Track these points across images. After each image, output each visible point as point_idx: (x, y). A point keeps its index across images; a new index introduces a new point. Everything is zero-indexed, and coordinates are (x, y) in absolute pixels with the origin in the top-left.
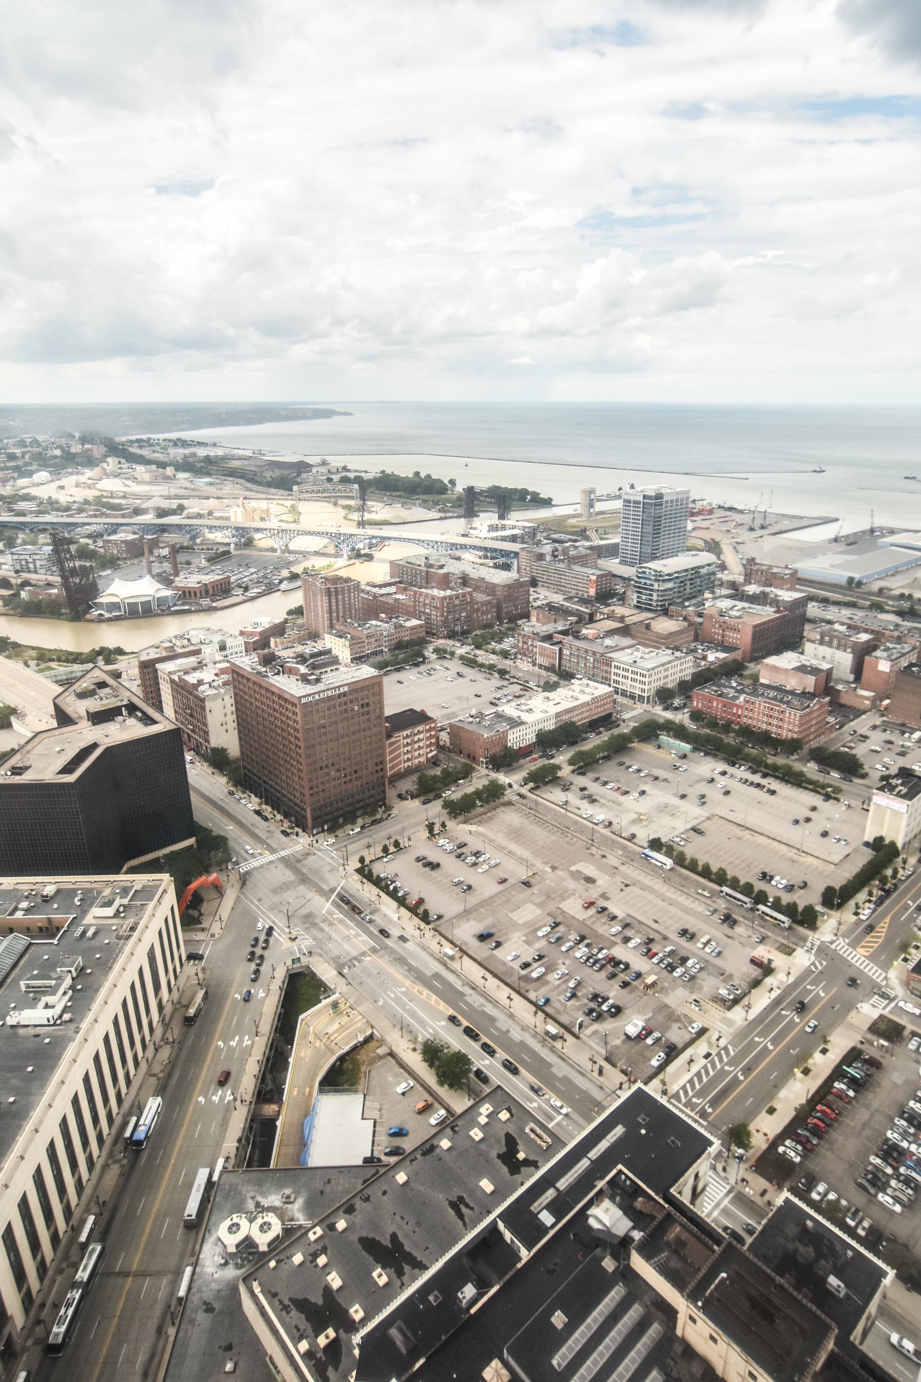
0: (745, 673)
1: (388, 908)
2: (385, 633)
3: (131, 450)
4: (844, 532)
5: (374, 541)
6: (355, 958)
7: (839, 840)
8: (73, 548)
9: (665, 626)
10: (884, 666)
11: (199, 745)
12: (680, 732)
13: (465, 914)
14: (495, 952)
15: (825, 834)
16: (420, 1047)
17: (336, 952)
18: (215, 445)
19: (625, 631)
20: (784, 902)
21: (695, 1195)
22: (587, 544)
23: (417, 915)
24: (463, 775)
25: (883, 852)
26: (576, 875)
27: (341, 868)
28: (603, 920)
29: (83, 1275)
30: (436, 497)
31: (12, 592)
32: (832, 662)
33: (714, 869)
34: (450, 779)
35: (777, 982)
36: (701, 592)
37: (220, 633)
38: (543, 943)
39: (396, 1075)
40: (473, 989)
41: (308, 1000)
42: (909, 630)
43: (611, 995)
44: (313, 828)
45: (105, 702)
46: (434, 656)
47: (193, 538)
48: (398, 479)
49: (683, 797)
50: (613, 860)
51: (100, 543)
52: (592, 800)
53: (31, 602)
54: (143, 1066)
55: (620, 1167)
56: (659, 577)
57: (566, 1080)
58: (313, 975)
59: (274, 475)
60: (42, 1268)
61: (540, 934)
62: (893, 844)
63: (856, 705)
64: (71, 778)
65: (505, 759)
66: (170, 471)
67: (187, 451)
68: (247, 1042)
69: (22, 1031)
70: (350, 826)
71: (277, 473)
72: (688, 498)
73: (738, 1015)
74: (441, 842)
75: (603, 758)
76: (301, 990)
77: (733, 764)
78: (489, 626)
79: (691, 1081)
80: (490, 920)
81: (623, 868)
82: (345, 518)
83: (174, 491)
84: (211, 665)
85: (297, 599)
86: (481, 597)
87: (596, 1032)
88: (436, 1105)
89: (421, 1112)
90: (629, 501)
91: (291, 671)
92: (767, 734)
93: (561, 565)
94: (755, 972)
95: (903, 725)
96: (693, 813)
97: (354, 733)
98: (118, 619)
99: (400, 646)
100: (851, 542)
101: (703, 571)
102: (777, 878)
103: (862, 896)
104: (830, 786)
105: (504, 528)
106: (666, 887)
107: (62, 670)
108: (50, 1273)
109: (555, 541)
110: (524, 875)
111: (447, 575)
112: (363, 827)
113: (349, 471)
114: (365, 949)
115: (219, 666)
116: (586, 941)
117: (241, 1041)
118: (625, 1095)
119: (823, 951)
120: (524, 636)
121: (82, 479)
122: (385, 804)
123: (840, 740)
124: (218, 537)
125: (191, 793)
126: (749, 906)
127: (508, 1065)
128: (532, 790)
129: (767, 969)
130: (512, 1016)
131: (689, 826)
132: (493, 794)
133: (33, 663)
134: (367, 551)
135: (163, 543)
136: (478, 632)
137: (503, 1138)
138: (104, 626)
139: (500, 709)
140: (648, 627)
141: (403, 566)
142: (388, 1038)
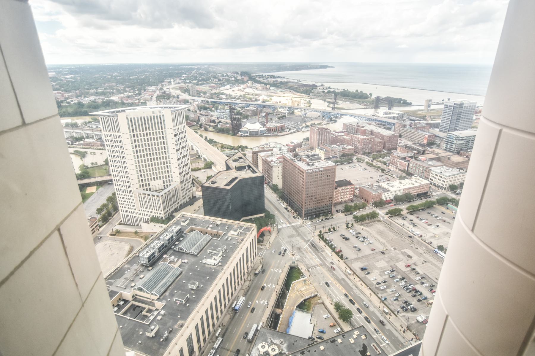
1: (328, 250)
6: (314, 266)
8: (235, 111)
13: (357, 259)
14: (367, 276)
16: (334, 304)
17: (308, 263)
18: (284, 78)
23: (338, 256)
24: (362, 208)
26: (404, 254)
29: (216, 346)
34: (357, 207)
39: (324, 311)
41: (296, 277)
46: (356, 161)
47: (274, 110)
50: (420, 251)
51: (244, 110)
52: (414, 225)
54: (240, 286)
58: (299, 269)
60: (205, 340)
61: (386, 273)
64: (229, 188)
65: (380, 204)
66: (268, 86)
67: (275, 80)
68: (274, 286)
69: (207, 265)
74: (351, 231)
75: (422, 209)
76: (293, 273)
78: (380, 151)
80: (366, 264)
81: (424, 255)
82: (328, 106)
83: (269, 94)
84: (276, 155)
85: (307, 135)
87: (404, 316)
88: (337, 326)
89: (331, 327)
91: (303, 160)
98: (247, 136)
99: (343, 155)
107: (228, 151)
108: (207, 342)
110: (382, 249)
111: (365, 130)
112: (322, 220)
114: (318, 264)
117: (272, 286)
120: (394, 157)
121: (240, 88)
124: (282, 110)
127: (366, 319)
128: (389, 217)
130: (370, 301)
132: (373, 216)
133: (220, 148)
135: (265, 112)
136: (375, 153)
138: (242, 138)
139: (380, 184)
142: (322, 297)
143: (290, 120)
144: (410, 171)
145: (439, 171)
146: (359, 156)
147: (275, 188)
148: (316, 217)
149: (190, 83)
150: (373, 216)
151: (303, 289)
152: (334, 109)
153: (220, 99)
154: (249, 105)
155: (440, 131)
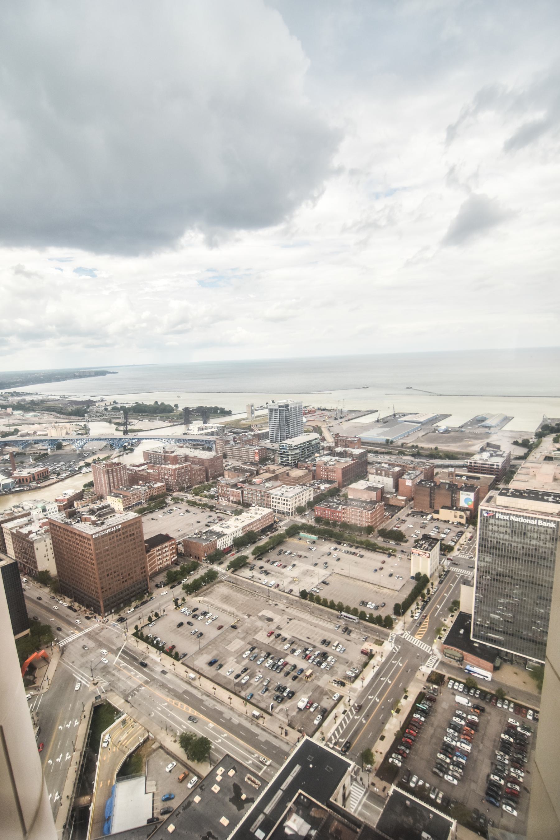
0: (341, 494)
1: (154, 655)
2: (143, 492)
4: (381, 417)
7: (398, 577)
9: (296, 473)
10: (409, 483)
11: (31, 571)
14: (219, 671)
15: (391, 575)
16: (178, 739)
19: (276, 478)
20: (375, 616)
21: (345, 799)
22: (252, 433)
23: (171, 656)
25: (421, 581)
26: (261, 618)
27: (124, 634)
28: (280, 642)
30: (168, 414)
32: (383, 483)
33: (336, 603)
34: (186, 572)
35: (377, 661)
36: (313, 453)
37: (43, 502)
38: (247, 661)
39: (165, 760)
40: (208, 696)
42: (418, 463)
43: (288, 686)
44: (105, 612)
46: (172, 502)
48: (146, 406)
49: (316, 565)
50: (281, 606)
52: (267, 573)
55: (300, 791)
56: (291, 448)
57: (267, 743)
58: (109, 705)
59: (73, 409)
61: (244, 656)
62: (425, 576)
63: (398, 505)
65: (217, 556)
66: (9, 410)
67: (19, 398)
68: (68, 757)
70: (127, 608)
71: (75, 407)
72: (302, 406)
73: (358, 685)
77: (340, 543)
79: (337, 729)
80: (215, 652)
81: (287, 610)
83: (12, 422)
84: (36, 521)
85: (90, 478)
86: (196, 467)
87: (281, 710)
88: (191, 774)
89: (181, 781)
90: (272, 409)
92: (355, 525)
93: (239, 446)
94: (364, 658)
95: (422, 512)
96: (321, 573)
97: (126, 552)
99: (152, 498)
100: (384, 422)
101: (313, 443)
102: (370, 603)
103: (413, 607)
104: (390, 549)
105: (206, 428)
106: (312, 617)
109: (235, 433)
110: (233, 622)
111: (176, 457)
112: (136, 608)
113: (117, 403)
114: (141, 682)
115: (42, 521)
116: (271, 656)
118: (299, 745)
119: (398, 640)
120: (222, 486)
122: (148, 592)
123: (391, 524)
125: (26, 600)
126: (357, 621)
128: (233, 572)
129: (370, 655)
130: (232, 709)
131: (320, 581)
132: (211, 577)
134: (129, 447)
136: (196, 486)
137: (232, 787)
139: (211, 528)
140: (288, 474)
141: (151, 454)
142: (159, 737)
143: (56, 459)
144: (247, 500)
145: (279, 493)
146: (175, 494)
147: (43, 578)
148: (125, 606)
150: (211, 577)
151: (122, 738)
152: (126, 432)
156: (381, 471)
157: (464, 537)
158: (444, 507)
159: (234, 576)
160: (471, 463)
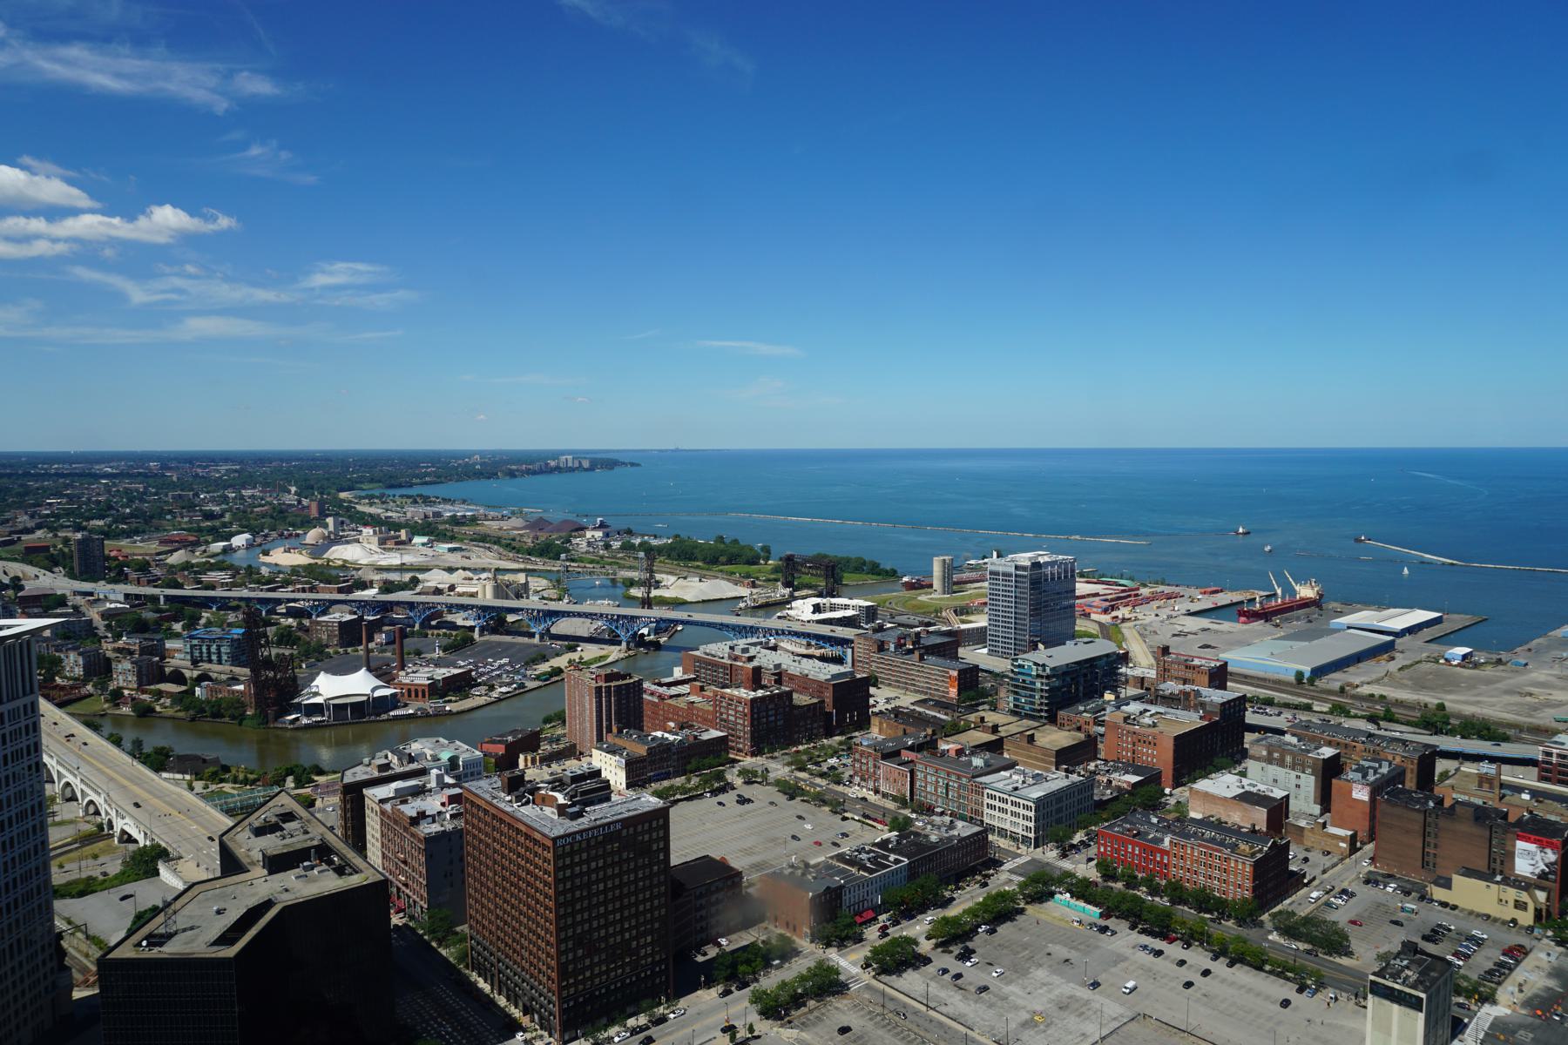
3: (359, 508)
5: (663, 625)
8: (271, 631)
12: (1082, 890)
18: (464, 502)
30: (746, 568)
31: (184, 688)
45: (288, 841)
53: (208, 701)
64: (231, 952)
66: (403, 534)
67: (429, 510)
86: (801, 699)
90: (997, 573)
91: (546, 801)
105: (833, 608)
111: (757, 671)
135: (388, 627)
140: (1031, 739)
149: (78, 528)
153: (206, 588)
154: (325, 607)
155: (991, 653)
156: (1283, 753)
157: (1528, 962)
158: (1470, 873)
159: (882, 986)
160: (1549, 754)
